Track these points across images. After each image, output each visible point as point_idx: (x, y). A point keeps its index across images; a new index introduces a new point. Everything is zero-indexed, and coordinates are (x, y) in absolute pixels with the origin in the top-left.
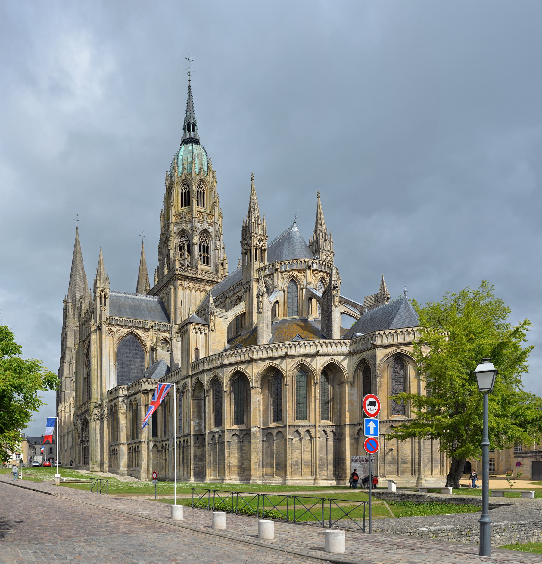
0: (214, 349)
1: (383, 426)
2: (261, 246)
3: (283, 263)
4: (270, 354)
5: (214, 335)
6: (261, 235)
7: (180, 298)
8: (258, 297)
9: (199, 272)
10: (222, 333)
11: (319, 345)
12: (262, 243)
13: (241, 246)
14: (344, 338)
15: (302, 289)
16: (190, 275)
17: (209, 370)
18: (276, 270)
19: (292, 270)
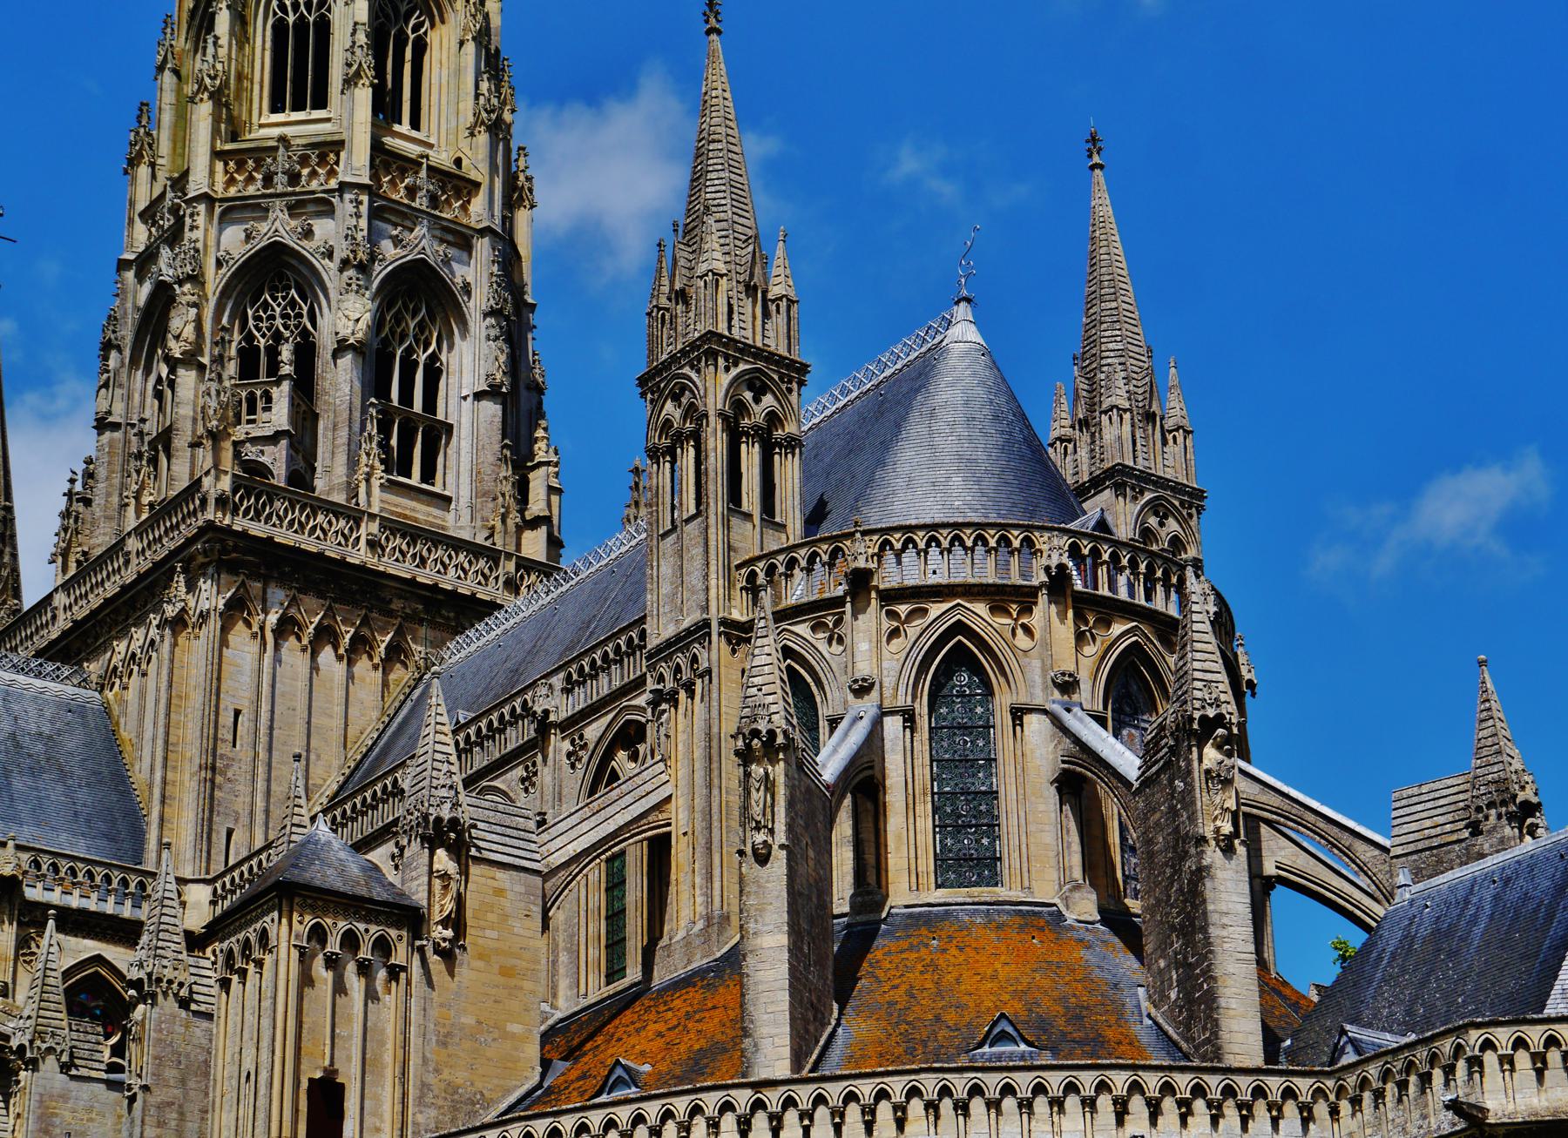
0: (452, 1089)
7: (238, 691)
8: (746, 757)
9: (369, 528)
10: (506, 972)
12: (768, 400)
15: (1018, 714)
16: (309, 544)
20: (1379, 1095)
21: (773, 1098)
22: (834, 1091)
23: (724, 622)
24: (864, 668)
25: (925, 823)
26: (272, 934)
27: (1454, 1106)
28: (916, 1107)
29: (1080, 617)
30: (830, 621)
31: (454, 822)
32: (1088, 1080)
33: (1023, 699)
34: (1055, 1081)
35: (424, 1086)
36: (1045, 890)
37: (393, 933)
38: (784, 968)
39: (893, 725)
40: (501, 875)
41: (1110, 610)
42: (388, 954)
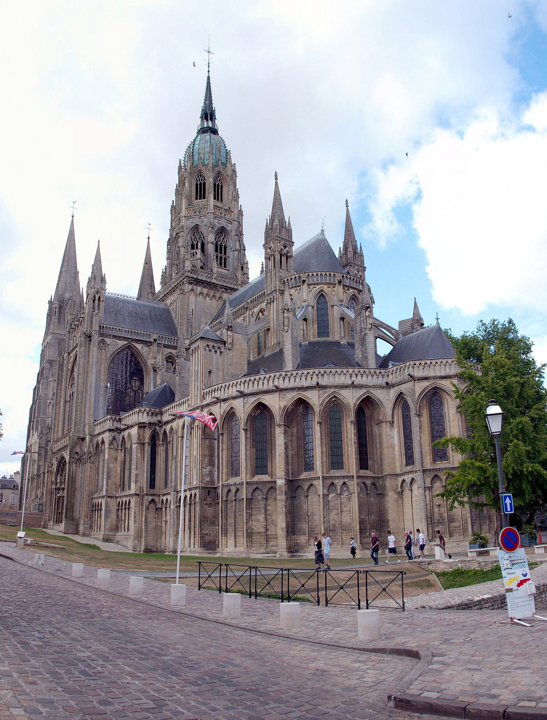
0: (232, 373)
1: (428, 476)
2: (286, 252)
3: (311, 274)
4: (299, 383)
5: (231, 355)
6: (287, 240)
10: (241, 353)
11: (354, 376)
13: (263, 251)
14: (380, 367)
15: (333, 306)
17: (225, 400)
18: (304, 281)
19: (320, 284)
20: (396, 373)
21: (289, 374)
22: (300, 372)
23: (279, 290)
24: (305, 298)
25: (316, 326)
26: (200, 346)
27: (409, 375)
28: (315, 376)
29: (344, 288)
30: (298, 289)
31: (231, 326)
32: (345, 371)
33: (333, 304)
34: (339, 370)
35: (227, 373)
36: (337, 338)
37: (221, 346)
38: (291, 351)
39: (310, 308)
40: (240, 336)
41: (350, 287)
42: (220, 349)
